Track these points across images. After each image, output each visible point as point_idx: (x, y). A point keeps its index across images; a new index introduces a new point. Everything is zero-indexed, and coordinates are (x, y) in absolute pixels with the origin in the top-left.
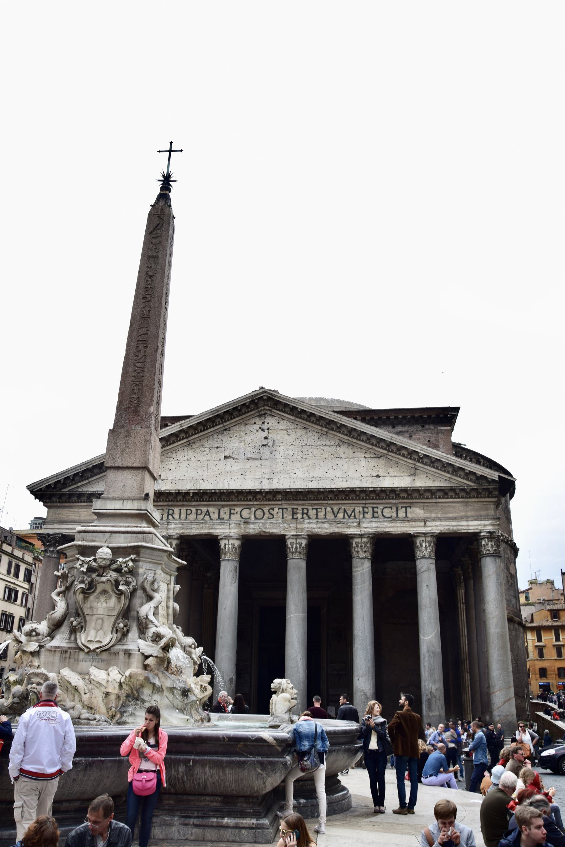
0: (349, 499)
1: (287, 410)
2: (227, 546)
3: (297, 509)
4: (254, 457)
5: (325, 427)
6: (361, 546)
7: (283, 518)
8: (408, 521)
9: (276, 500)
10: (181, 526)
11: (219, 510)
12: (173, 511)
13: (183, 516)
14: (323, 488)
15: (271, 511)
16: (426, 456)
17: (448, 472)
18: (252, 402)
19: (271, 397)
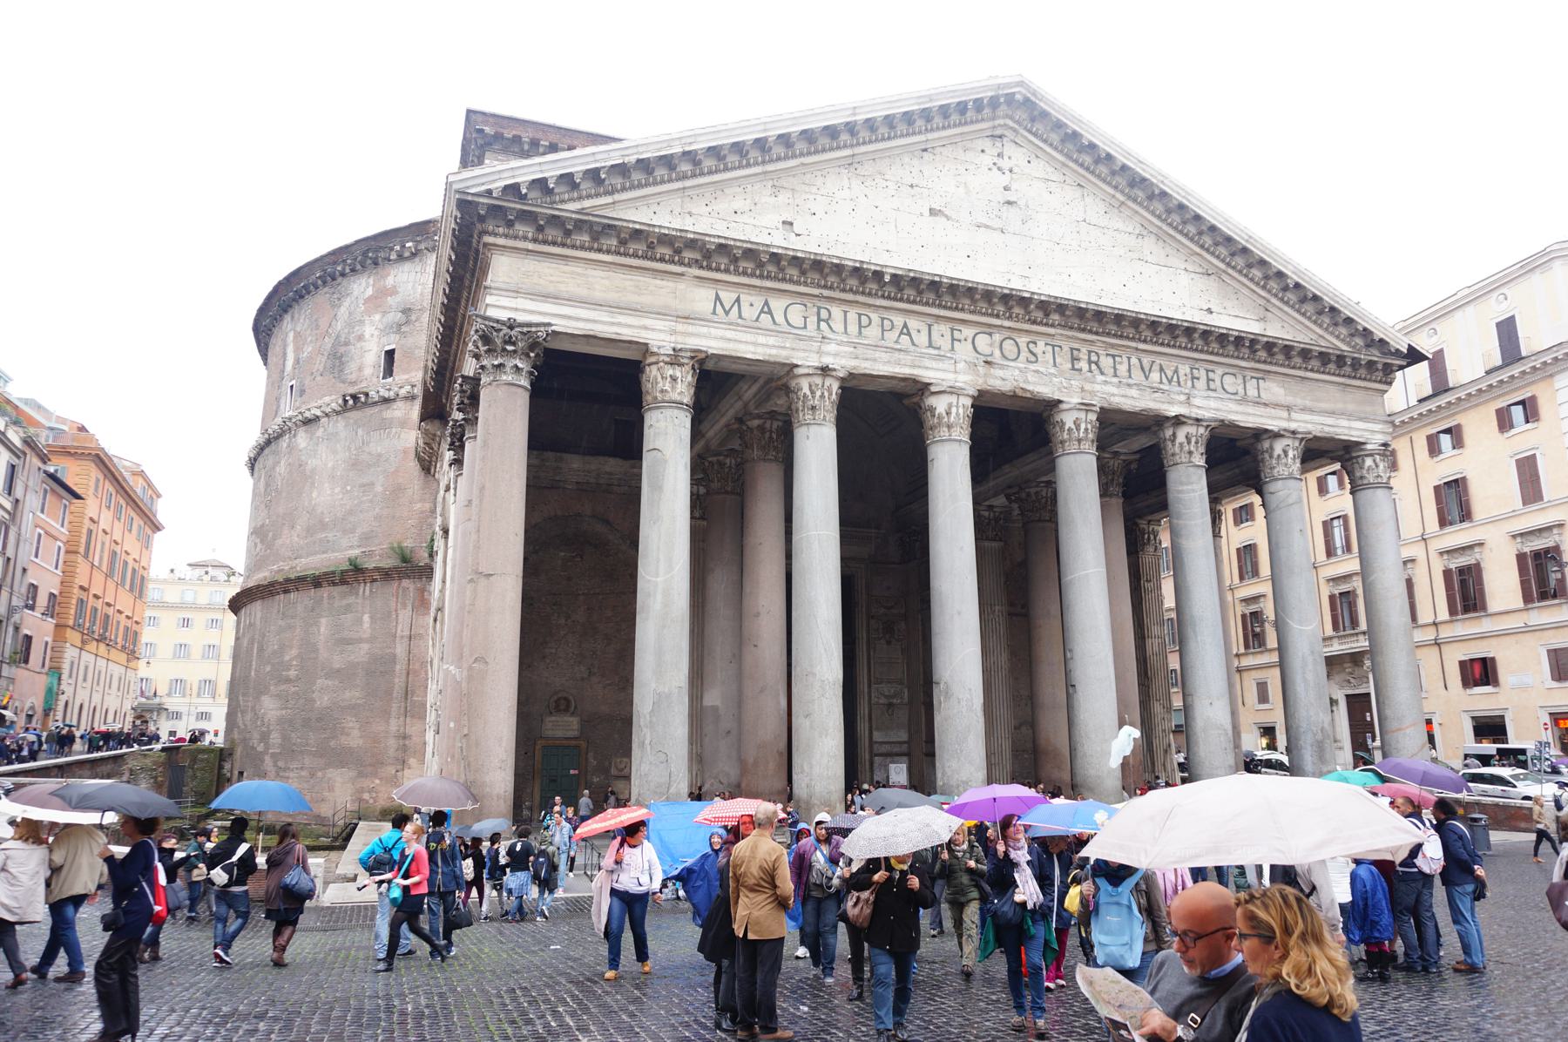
0: (1174, 346)
1: (1055, 137)
2: (954, 410)
3: (1078, 350)
5: (1122, 192)
6: (1197, 443)
7: (1055, 365)
8: (1265, 405)
9: (1046, 325)
11: (930, 326)
13: (853, 328)
14: (1145, 314)
15: (1031, 345)
16: (1297, 286)
17: (1320, 326)
18: (992, 97)
19: (1033, 98)
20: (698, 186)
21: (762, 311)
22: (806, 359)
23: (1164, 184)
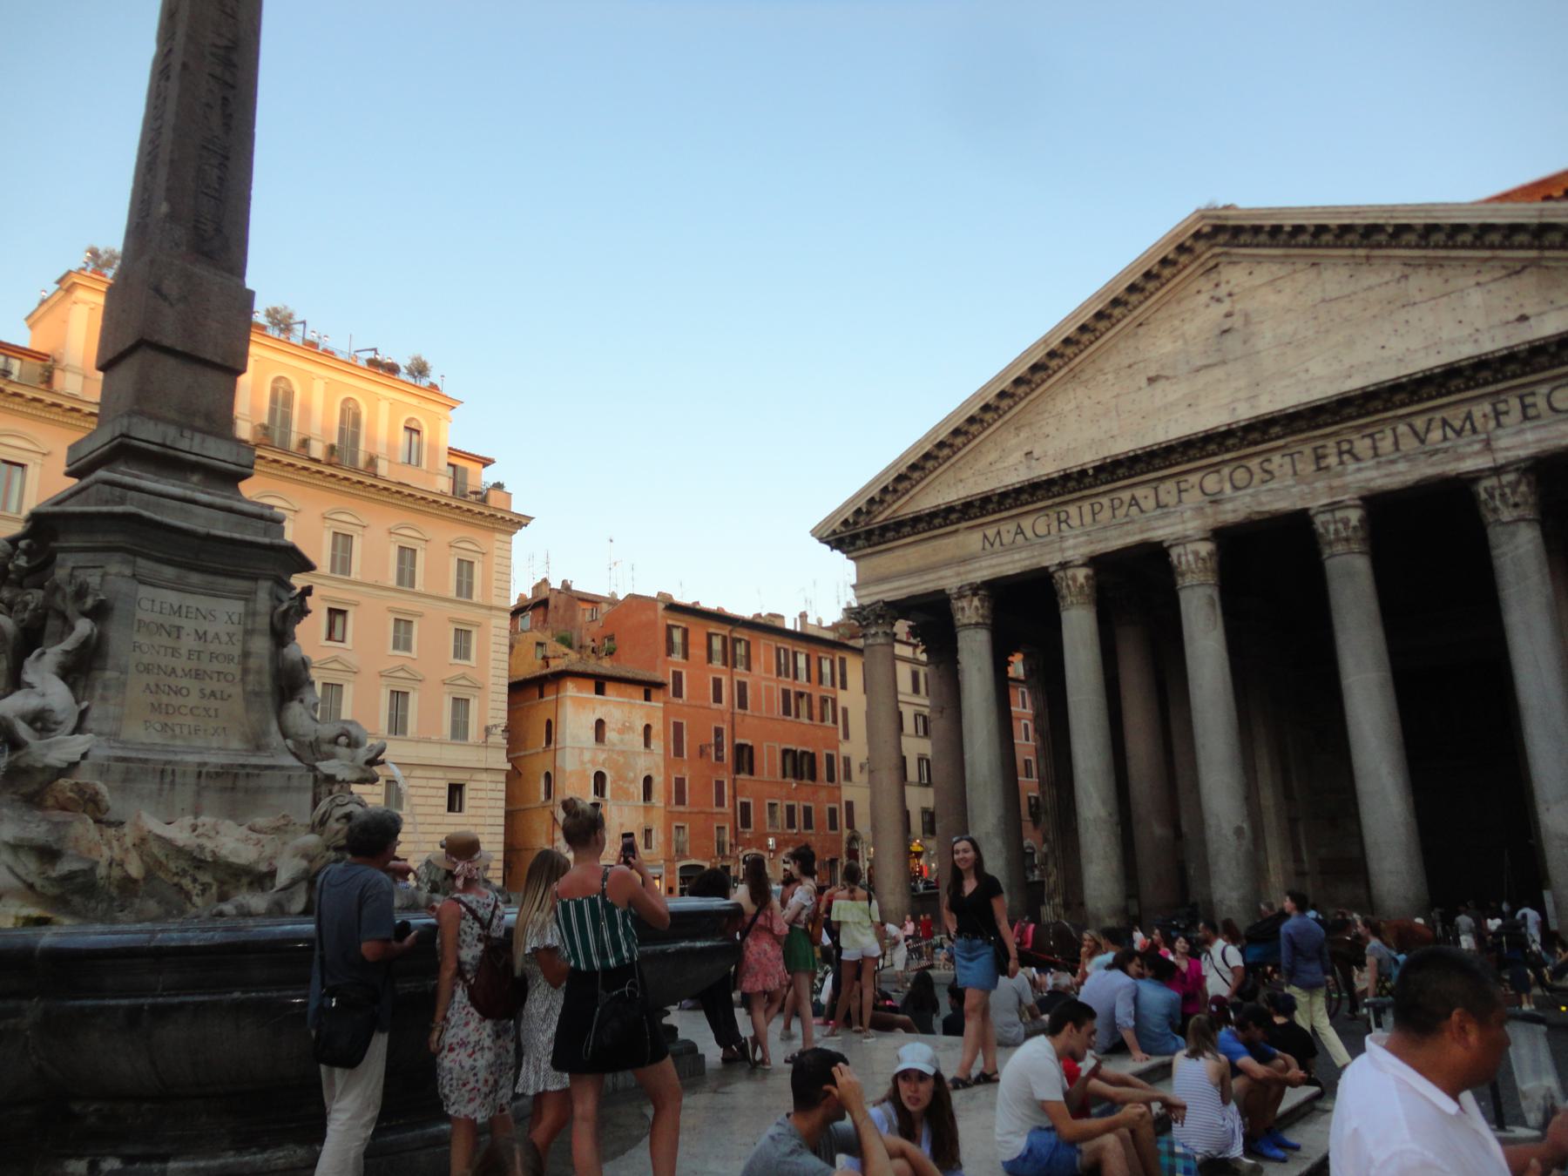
0: (1449, 393)
1: (1263, 238)
2: (1183, 559)
3: (1323, 447)
4: (1210, 361)
5: (1360, 246)
6: (1503, 495)
7: (1295, 473)
9: (1271, 440)
10: (1082, 539)
11: (1156, 489)
12: (1067, 512)
13: (1088, 518)
15: (1266, 465)
18: (1181, 249)
19: (1219, 222)
20: (962, 457)
21: (1017, 534)
22: (1050, 560)
23: (1397, 218)
